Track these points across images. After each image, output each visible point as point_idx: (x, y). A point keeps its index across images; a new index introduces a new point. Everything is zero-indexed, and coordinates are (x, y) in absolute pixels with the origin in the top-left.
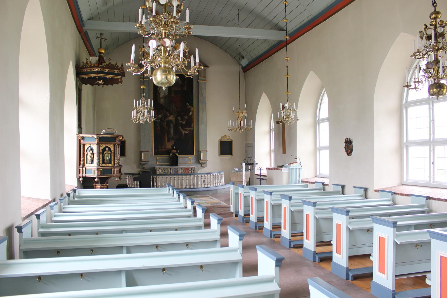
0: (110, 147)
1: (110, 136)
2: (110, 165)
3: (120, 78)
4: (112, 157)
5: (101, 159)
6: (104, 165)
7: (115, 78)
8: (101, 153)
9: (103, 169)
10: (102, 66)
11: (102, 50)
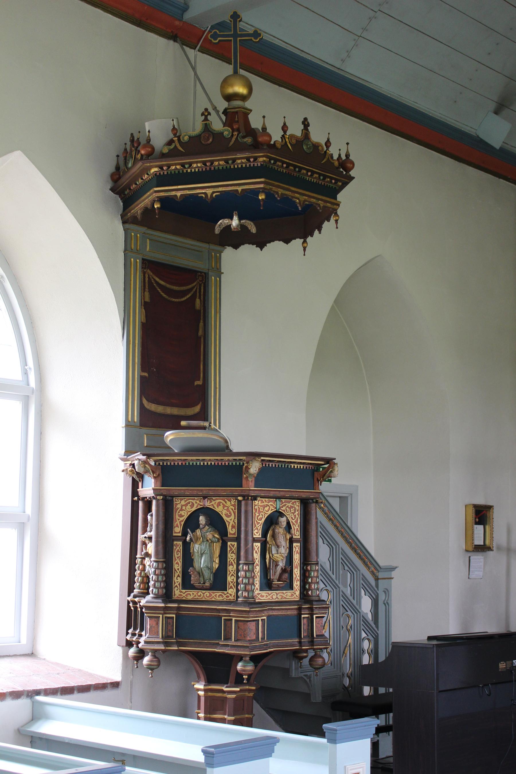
0: (218, 509)
1: (210, 460)
2: (217, 595)
3: (262, 186)
4: (297, 557)
5: (178, 566)
6: (191, 595)
7: (240, 189)
8: (177, 538)
9: (176, 614)
10: (170, 151)
11: (232, 86)
